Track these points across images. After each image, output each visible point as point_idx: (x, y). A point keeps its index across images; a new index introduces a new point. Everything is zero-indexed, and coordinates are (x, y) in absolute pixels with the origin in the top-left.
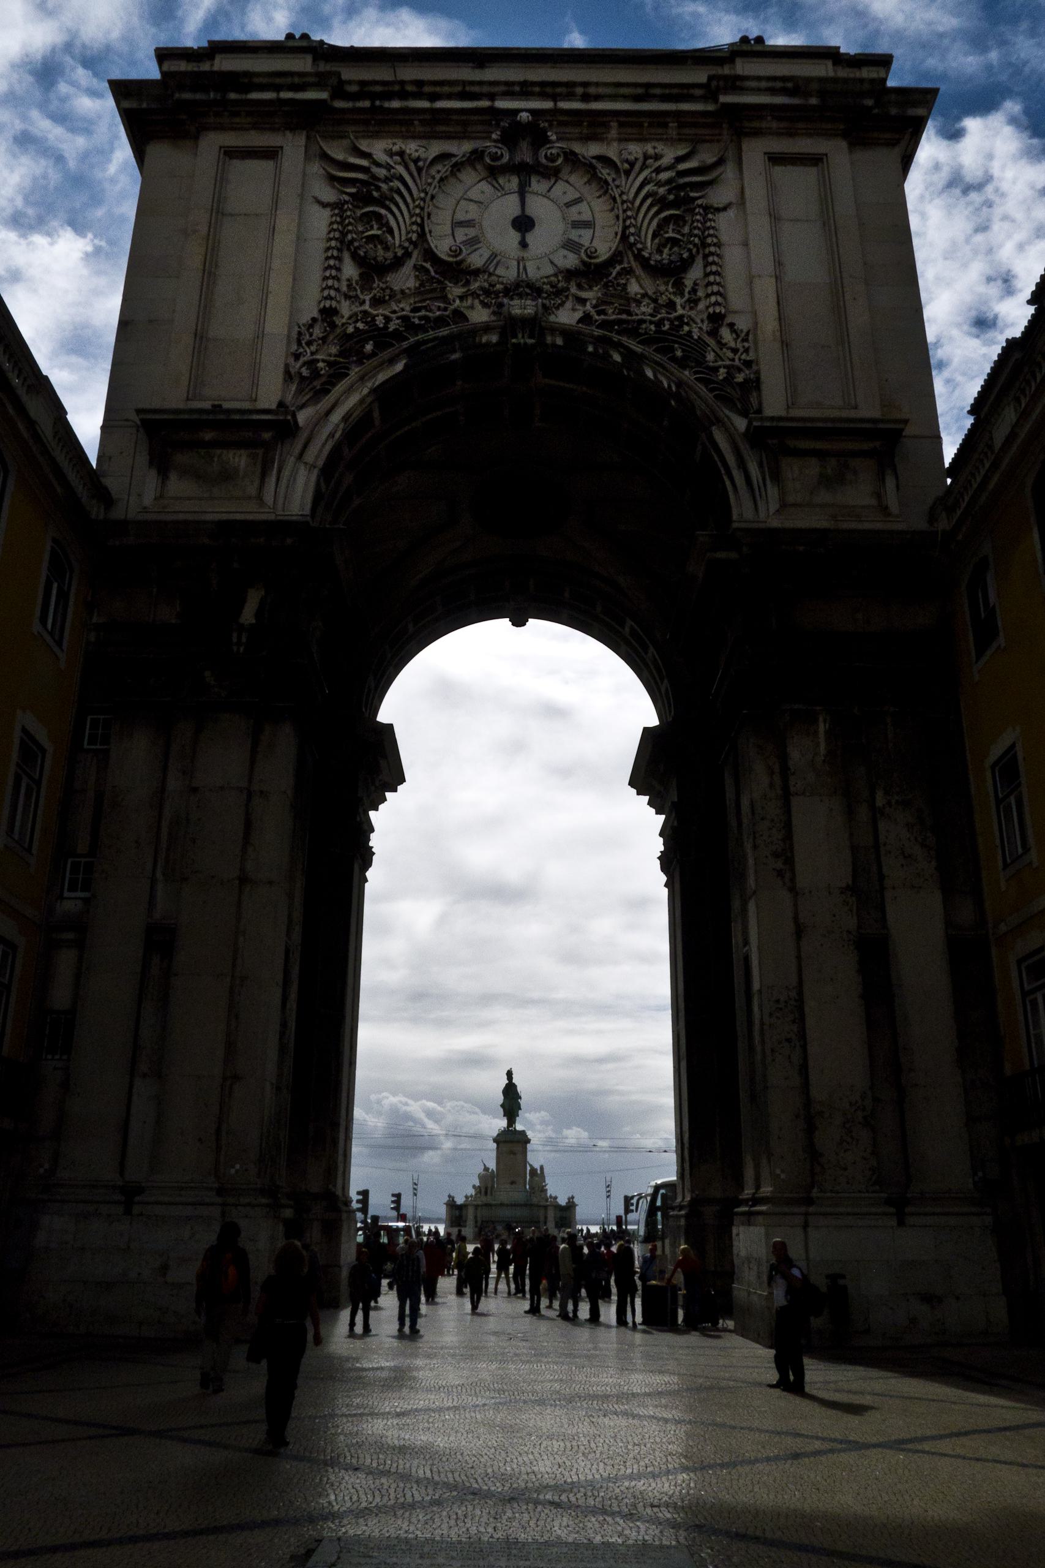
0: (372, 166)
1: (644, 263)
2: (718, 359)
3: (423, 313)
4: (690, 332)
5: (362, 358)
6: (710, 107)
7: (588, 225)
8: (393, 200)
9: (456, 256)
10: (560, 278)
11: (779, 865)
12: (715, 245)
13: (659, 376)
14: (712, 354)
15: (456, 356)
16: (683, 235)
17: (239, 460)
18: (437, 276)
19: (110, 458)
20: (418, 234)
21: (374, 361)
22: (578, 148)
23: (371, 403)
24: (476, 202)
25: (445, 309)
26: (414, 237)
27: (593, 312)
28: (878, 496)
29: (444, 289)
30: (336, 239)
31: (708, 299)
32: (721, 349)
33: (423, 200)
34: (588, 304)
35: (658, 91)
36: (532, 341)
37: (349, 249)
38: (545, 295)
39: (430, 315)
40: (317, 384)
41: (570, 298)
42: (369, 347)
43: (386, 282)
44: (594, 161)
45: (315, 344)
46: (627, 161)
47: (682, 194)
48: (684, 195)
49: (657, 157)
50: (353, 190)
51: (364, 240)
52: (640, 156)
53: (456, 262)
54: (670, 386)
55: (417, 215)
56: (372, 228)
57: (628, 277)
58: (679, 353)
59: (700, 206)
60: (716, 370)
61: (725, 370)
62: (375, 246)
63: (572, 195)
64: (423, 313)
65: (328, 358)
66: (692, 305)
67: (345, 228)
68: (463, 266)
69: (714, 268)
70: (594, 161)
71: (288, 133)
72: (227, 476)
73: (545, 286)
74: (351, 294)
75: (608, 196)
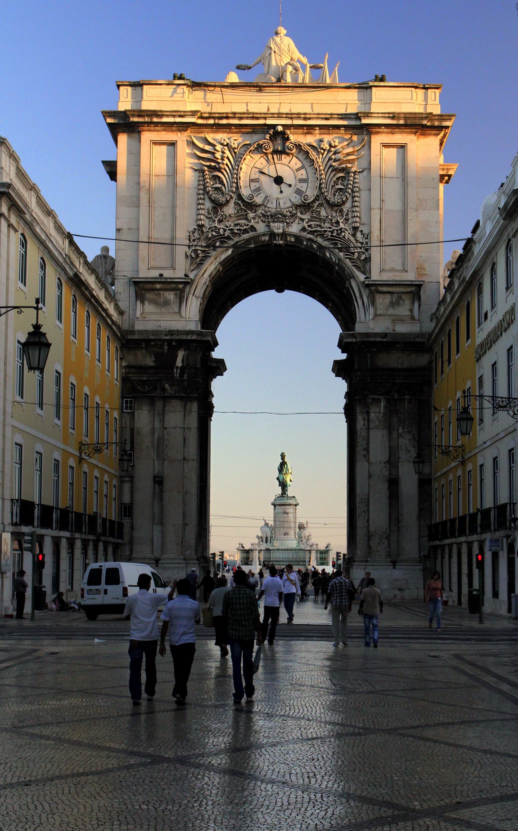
3: (238, 227)
4: (345, 235)
5: (215, 248)
6: (358, 123)
11: (365, 453)
13: (332, 256)
15: (252, 246)
16: (344, 186)
17: (171, 296)
19: (120, 293)
21: (219, 250)
25: (248, 225)
28: (411, 310)
29: (246, 215)
35: (336, 116)
39: (242, 228)
42: (218, 244)
43: (223, 212)
46: (322, 149)
49: (336, 146)
50: (208, 164)
54: (335, 260)
56: (216, 183)
60: (353, 253)
64: (238, 227)
71: (178, 133)
72: (167, 303)
74: (210, 216)
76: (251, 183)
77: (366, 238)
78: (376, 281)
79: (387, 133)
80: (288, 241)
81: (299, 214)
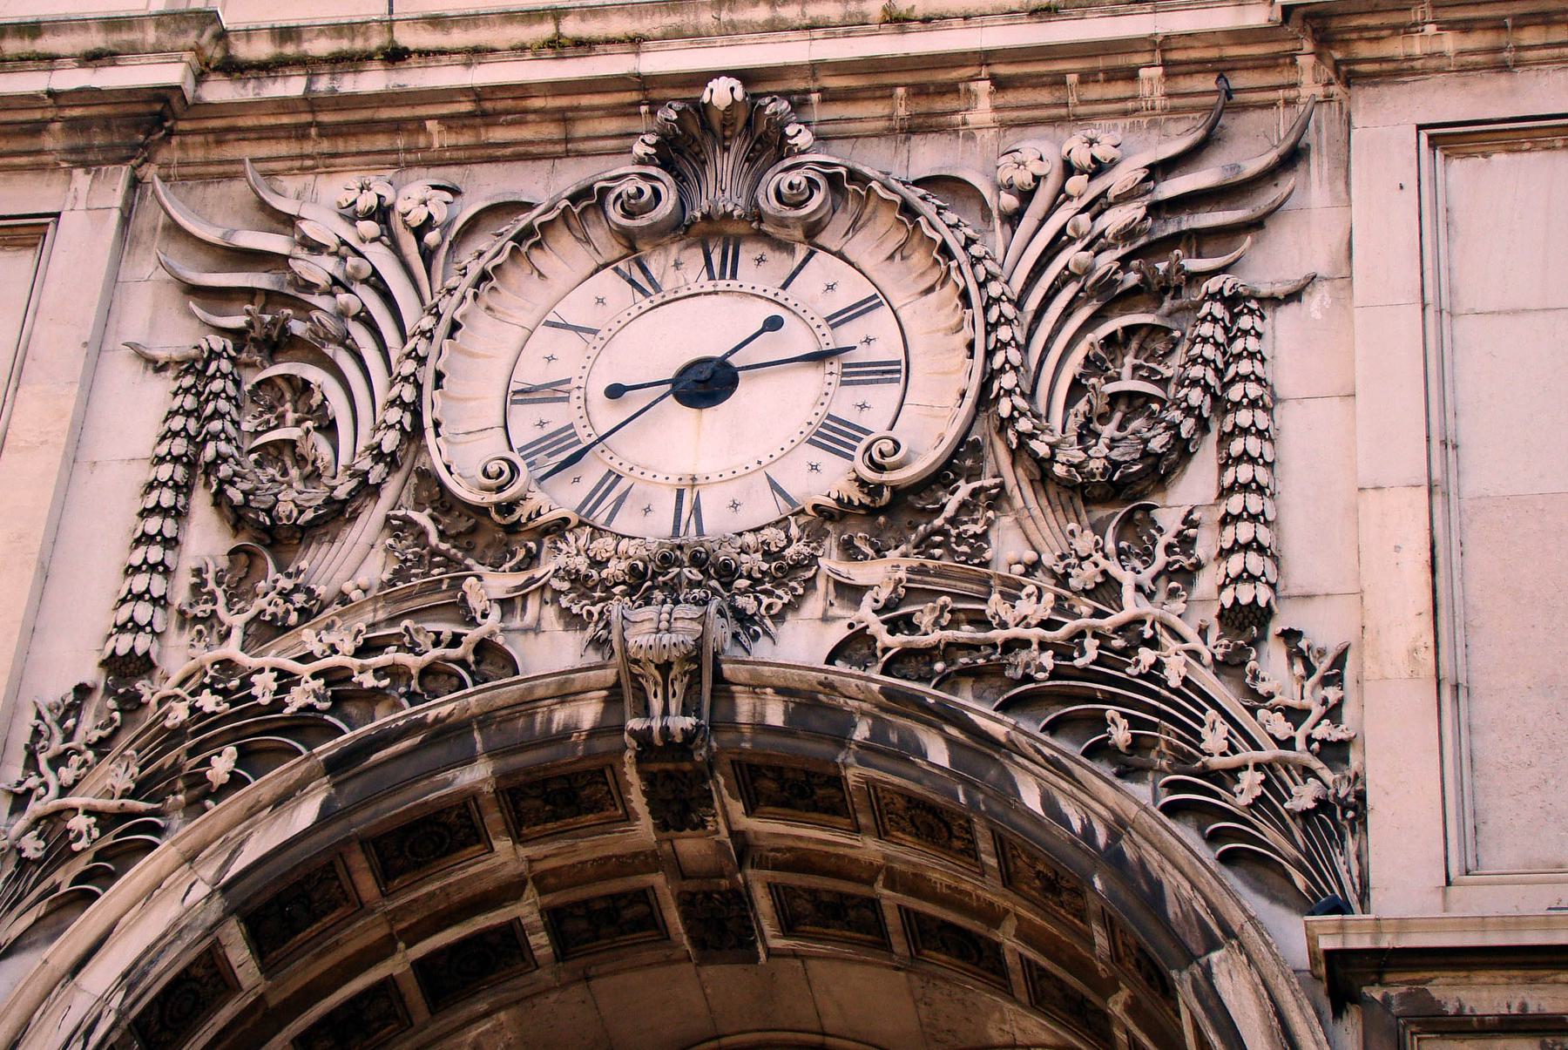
0: (301, 253)
1: (1041, 476)
2: (1240, 742)
4: (1158, 665)
5: (202, 794)
7: (894, 372)
8: (345, 341)
9: (500, 489)
10: (794, 531)
12: (1253, 404)
14: (1223, 728)
15: (477, 774)
18: (444, 546)
20: (403, 429)
21: (235, 803)
22: (873, 160)
23: (219, 922)
24: (577, 329)
25: (456, 641)
26: (390, 441)
27: (877, 627)
29: (456, 583)
30: (176, 460)
31: (1223, 565)
32: (1253, 711)
33: (428, 335)
34: (867, 599)
36: (689, 722)
37: (207, 484)
38: (743, 583)
40: (64, 878)
41: (821, 583)
42: (222, 765)
43: (299, 572)
44: (914, 194)
45: (75, 760)
46: (1009, 187)
47: (1162, 266)
48: (1168, 271)
49: (1098, 168)
51: (254, 456)
52: (1052, 169)
53: (498, 505)
54: (1088, 833)
55: (406, 379)
57: (990, 514)
58: (1121, 734)
59: (1212, 297)
60: (1234, 772)
61: (1260, 777)
62: (285, 473)
63: (852, 289)
65: (101, 803)
66: (1174, 584)
67: (203, 426)
68: (522, 513)
69: (1244, 472)
70: (914, 194)
71: (79, 173)
73: (744, 557)
74: (201, 610)
75: (949, 287)
76: (515, 410)
77: (1326, 681)
78: (1402, 925)
79: (1463, 69)
80: (734, 726)
81: (831, 562)
